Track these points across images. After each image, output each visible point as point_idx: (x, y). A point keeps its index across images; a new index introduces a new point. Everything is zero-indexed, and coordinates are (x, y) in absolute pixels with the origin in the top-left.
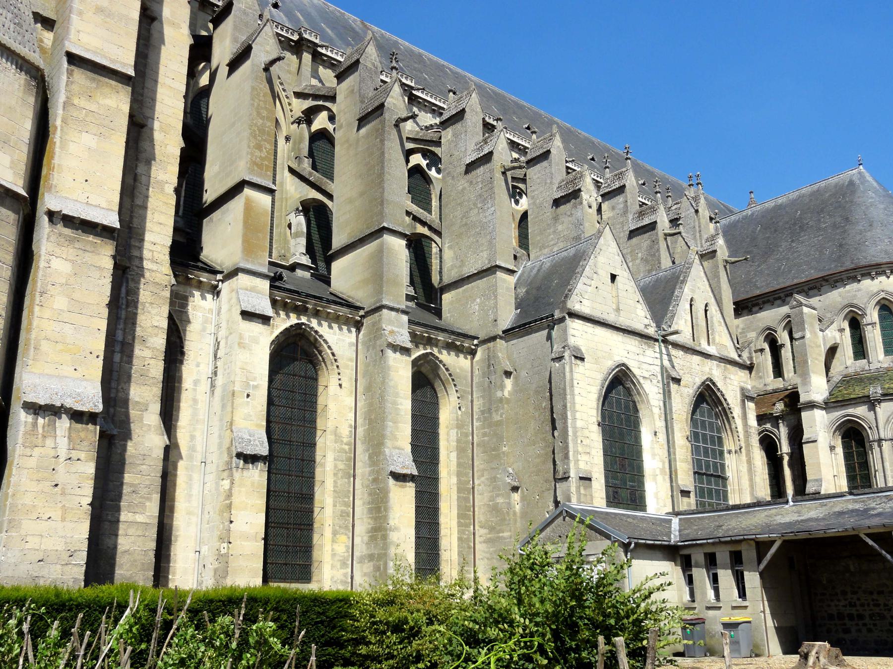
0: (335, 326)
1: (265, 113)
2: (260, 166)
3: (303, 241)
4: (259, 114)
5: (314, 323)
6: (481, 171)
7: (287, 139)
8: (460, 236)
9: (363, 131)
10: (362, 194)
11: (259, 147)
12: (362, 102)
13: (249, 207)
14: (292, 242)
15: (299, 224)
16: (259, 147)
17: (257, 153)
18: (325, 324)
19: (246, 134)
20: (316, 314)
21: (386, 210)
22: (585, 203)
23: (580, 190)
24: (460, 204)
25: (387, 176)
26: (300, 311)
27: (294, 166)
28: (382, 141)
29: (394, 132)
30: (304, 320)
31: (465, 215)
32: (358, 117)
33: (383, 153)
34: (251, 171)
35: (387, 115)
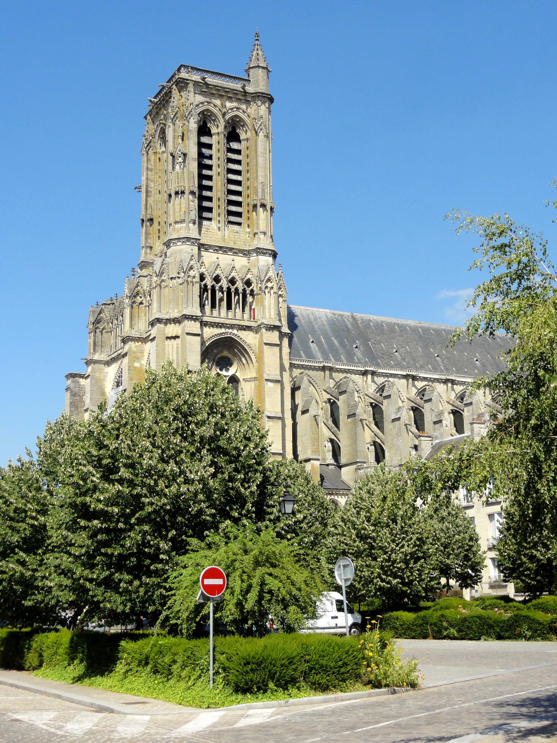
0: (343, 497)
1: (315, 432)
2: (315, 452)
3: (331, 453)
4: (313, 433)
5: (336, 497)
6: (397, 423)
7: (322, 409)
8: (391, 448)
9: (349, 420)
10: (350, 445)
11: (314, 445)
12: (348, 407)
13: (312, 465)
14: (327, 454)
15: (329, 447)
16: (314, 445)
17: (314, 447)
18: (340, 497)
19: (310, 441)
20: (336, 494)
21: (358, 455)
22: (444, 425)
23: (442, 420)
24: (391, 435)
25: (358, 441)
26: (331, 494)
27: (325, 422)
28: (356, 427)
29: (360, 423)
30: (332, 497)
31: (392, 440)
32: (347, 414)
33: (356, 433)
34: (312, 454)
35: (357, 417)
